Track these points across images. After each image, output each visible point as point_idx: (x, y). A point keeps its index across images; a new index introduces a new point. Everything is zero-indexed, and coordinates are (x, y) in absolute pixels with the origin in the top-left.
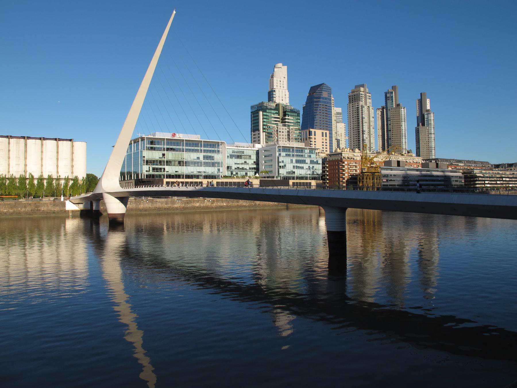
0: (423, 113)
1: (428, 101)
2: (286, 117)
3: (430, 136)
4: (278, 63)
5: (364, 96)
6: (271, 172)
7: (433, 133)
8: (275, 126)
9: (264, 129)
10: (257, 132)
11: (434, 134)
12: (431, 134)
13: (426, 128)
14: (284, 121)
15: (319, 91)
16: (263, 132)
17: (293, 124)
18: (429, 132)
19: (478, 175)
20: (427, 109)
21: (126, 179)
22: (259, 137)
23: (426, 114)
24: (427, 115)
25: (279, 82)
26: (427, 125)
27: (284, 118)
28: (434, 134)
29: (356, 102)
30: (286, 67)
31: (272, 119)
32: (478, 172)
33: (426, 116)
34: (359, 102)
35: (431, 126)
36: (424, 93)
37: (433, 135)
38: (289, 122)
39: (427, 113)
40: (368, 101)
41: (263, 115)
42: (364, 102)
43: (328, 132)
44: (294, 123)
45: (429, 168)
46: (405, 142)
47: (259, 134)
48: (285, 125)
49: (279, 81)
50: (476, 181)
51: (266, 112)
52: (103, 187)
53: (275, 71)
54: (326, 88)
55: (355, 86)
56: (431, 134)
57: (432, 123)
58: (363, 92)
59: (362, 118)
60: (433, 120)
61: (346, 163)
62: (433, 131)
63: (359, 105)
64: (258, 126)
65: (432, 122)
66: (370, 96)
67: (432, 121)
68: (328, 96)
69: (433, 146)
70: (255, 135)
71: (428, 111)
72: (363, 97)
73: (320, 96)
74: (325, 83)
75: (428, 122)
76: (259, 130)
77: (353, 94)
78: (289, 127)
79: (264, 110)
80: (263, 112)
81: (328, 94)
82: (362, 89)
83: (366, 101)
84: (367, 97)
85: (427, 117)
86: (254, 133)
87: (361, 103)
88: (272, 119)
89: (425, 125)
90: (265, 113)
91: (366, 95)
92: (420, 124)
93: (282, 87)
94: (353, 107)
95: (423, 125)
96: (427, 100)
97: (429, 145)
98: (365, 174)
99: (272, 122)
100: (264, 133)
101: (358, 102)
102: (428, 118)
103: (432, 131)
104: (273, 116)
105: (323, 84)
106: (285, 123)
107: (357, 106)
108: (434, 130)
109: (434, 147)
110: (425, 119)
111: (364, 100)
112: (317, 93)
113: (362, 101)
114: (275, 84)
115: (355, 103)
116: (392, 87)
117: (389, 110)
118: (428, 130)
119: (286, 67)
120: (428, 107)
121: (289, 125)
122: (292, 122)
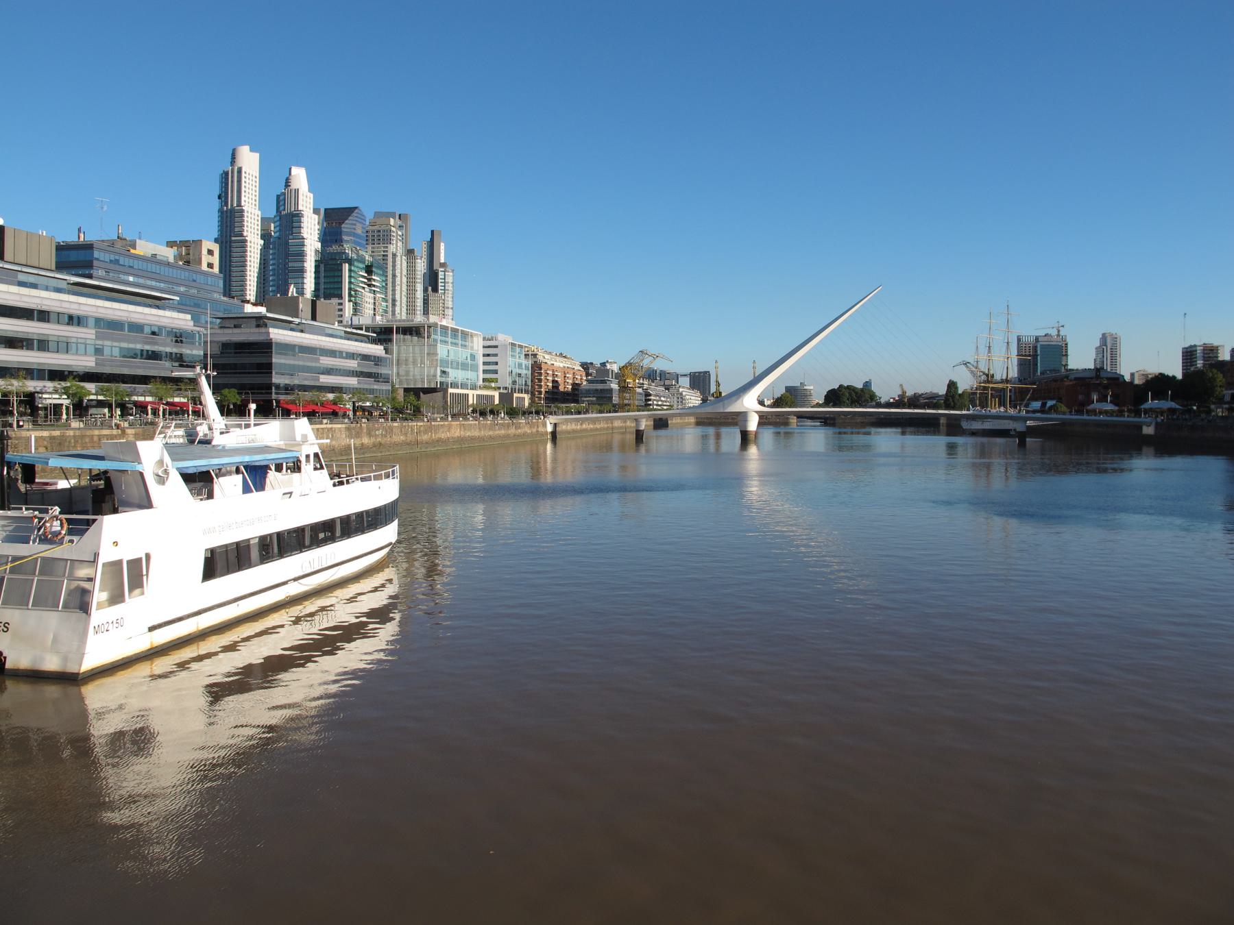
2: (373, 277)
3: (446, 313)
4: (242, 145)
7: (451, 306)
9: (350, 295)
10: (335, 301)
11: (452, 308)
12: (448, 308)
14: (369, 283)
15: (350, 222)
16: (350, 301)
22: (341, 310)
26: (443, 292)
28: (452, 308)
29: (381, 245)
30: (257, 155)
33: (441, 275)
34: (389, 245)
35: (448, 294)
37: (451, 310)
38: (374, 286)
39: (443, 269)
41: (350, 270)
42: (395, 245)
47: (341, 304)
54: (359, 216)
55: (376, 213)
56: (448, 308)
57: (451, 288)
59: (394, 276)
60: (452, 283)
62: (450, 303)
65: (450, 287)
67: (451, 285)
71: (443, 265)
73: (353, 231)
74: (361, 207)
75: (444, 286)
76: (340, 296)
77: (374, 228)
80: (350, 265)
85: (443, 277)
87: (392, 248)
89: (440, 291)
92: (430, 288)
95: (435, 290)
96: (442, 244)
100: (351, 303)
102: (444, 279)
103: (450, 304)
105: (356, 208)
107: (384, 251)
108: (453, 301)
110: (440, 281)
111: (395, 242)
112: (347, 224)
118: (444, 300)
119: (257, 155)
121: (374, 291)
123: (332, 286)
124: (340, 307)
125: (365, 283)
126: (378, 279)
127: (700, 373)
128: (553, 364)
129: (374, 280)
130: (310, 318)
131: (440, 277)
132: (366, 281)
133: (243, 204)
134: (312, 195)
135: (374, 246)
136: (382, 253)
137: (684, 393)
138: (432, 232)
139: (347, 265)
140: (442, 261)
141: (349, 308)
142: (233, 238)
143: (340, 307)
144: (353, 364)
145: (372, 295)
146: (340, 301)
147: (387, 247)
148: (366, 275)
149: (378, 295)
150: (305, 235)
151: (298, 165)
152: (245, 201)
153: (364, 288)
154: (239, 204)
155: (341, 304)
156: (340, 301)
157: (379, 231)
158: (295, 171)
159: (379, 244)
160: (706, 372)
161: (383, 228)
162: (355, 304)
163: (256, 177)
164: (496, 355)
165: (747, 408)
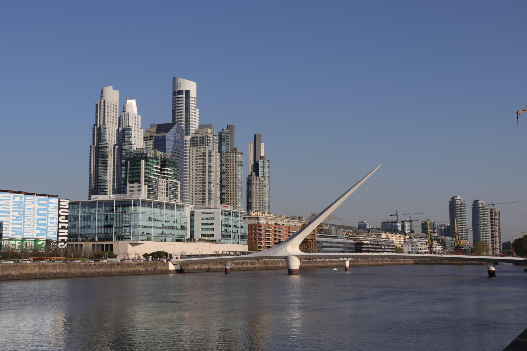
0: (257, 160)
1: (262, 145)
5: (211, 139)
6: (213, 235)
9: (146, 181)
10: (136, 184)
13: (261, 179)
14: (163, 172)
16: (145, 184)
17: (171, 177)
18: (264, 184)
19: (365, 242)
20: (262, 155)
21: (114, 240)
23: (260, 162)
24: (262, 163)
25: (134, 118)
30: (118, 92)
32: (383, 241)
36: (260, 136)
38: (167, 174)
40: (214, 145)
41: (146, 165)
43: (179, 182)
44: (172, 174)
45: (331, 235)
46: (242, 196)
47: (140, 187)
48: (164, 178)
49: (134, 117)
50: (363, 248)
51: (149, 161)
52: (289, 252)
53: (127, 103)
58: (210, 134)
61: (263, 227)
63: (205, 150)
64: (140, 176)
66: (216, 140)
68: (181, 139)
69: (267, 202)
70: (133, 187)
71: (262, 158)
72: (211, 140)
76: (139, 181)
78: (167, 180)
79: (146, 159)
80: (146, 161)
81: (181, 136)
82: (209, 131)
83: (213, 146)
84: (214, 141)
86: (132, 185)
90: (148, 163)
91: (213, 138)
93: (137, 125)
94: (197, 151)
96: (262, 144)
97: (263, 201)
98: (309, 240)
99: (154, 173)
100: (146, 186)
101: (205, 146)
104: (154, 166)
106: (164, 175)
107: (204, 150)
109: (269, 203)
111: (211, 144)
112: (169, 134)
113: (209, 146)
114: (130, 121)
115: (200, 147)
116: (228, 126)
117: (224, 154)
119: (118, 92)
120: (263, 154)
122: (170, 174)
124: (139, 189)
126: (171, 169)
131: (260, 166)
132: (160, 171)
133: (106, 123)
134: (140, 117)
135: (197, 147)
136: (203, 152)
137: (417, 243)
138: (255, 136)
139: (144, 161)
140: (263, 154)
141: (145, 189)
142: (100, 146)
143: (139, 189)
145: (165, 180)
146: (139, 185)
147: (205, 148)
149: (170, 180)
150: (133, 143)
151: (131, 98)
152: (108, 122)
154: (104, 124)
155: (140, 187)
156: (139, 185)
157: (201, 137)
158: (128, 101)
159: (201, 146)
161: (204, 135)
162: (149, 186)
163: (116, 106)
165: (290, 254)
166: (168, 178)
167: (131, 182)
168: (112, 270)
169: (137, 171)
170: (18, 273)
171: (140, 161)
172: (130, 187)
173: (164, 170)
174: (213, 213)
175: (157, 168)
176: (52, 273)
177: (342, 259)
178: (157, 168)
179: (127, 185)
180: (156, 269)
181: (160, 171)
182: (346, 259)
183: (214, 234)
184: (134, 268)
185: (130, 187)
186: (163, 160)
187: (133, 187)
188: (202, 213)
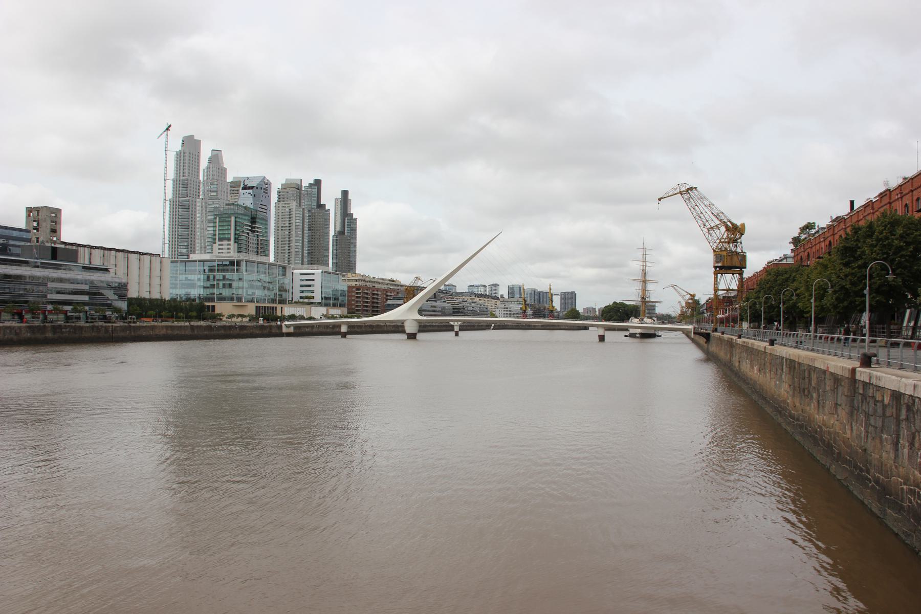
8: (247, 236)
10: (225, 242)
14: (254, 230)
27: (254, 226)
31: (245, 227)
38: (258, 232)
41: (236, 222)
70: (222, 245)
86: (221, 243)
88: (245, 227)
89: (346, 234)
100: (236, 244)
121: (258, 235)
123: (224, 232)
125: (249, 230)
127: (568, 293)
128: (374, 286)
129: (258, 228)
130: (50, 257)
132: (250, 228)
144: (86, 288)
146: (229, 243)
148: (250, 224)
153: (248, 234)
156: (229, 243)
160: (572, 293)
164: (313, 280)
166: (259, 236)
167: (220, 239)
168: (231, 332)
169: (227, 228)
170: (149, 334)
171: (230, 217)
172: (219, 245)
173: (254, 227)
174: (313, 274)
175: (248, 225)
176: (177, 334)
177: (452, 323)
178: (248, 225)
179: (215, 243)
180: (271, 332)
181: (250, 228)
182: (456, 323)
183: (314, 297)
184: (251, 331)
185: (219, 245)
186: (253, 217)
187: (222, 245)
188: (301, 274)
